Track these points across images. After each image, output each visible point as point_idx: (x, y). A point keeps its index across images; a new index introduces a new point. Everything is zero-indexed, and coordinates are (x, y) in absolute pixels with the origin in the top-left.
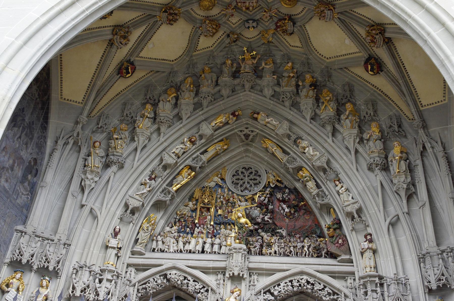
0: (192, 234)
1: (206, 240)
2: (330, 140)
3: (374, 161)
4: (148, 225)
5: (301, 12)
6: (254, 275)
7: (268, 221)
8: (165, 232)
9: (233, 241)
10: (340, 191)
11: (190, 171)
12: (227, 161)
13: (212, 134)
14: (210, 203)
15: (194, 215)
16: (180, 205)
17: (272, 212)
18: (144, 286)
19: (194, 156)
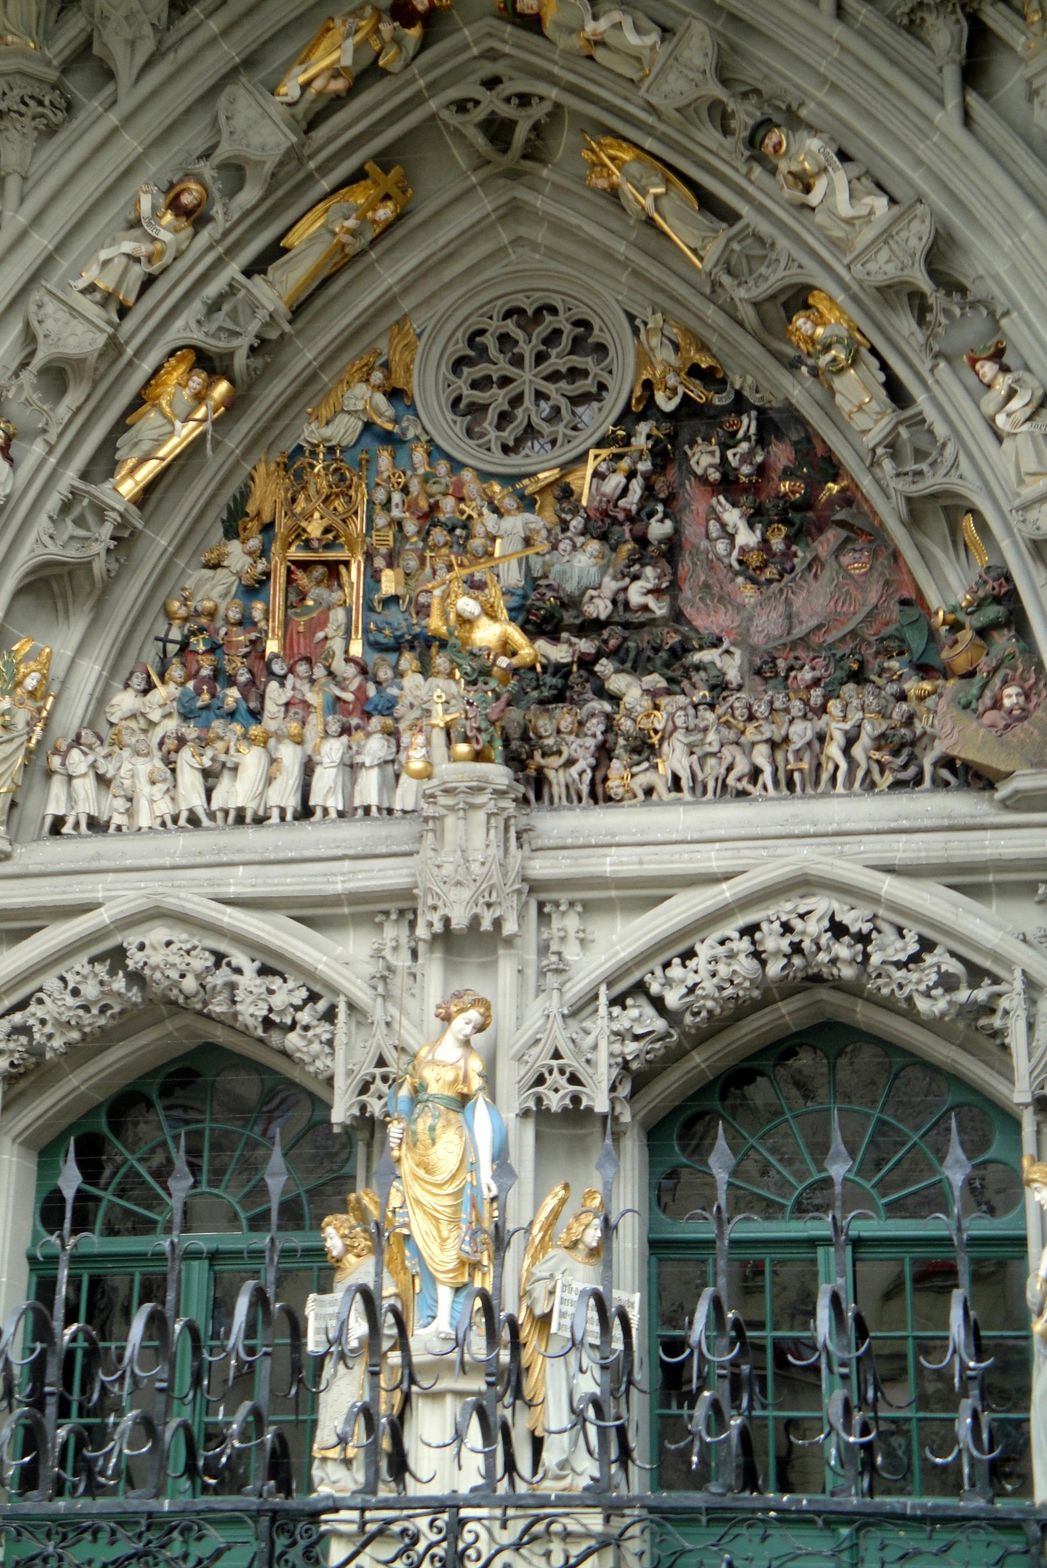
0: (256, 715)
1: (317, 750)
2: (948, 118)
6: (564, 913)
8: (114, 720)
10: (1001, 420)
11: (197, 380)
12: (408, 285)
13: (292, 148)
14: (336, 538)
15: (257, 614)
16: (181, 563)
18: (17, 1018)
19: (212, 290)
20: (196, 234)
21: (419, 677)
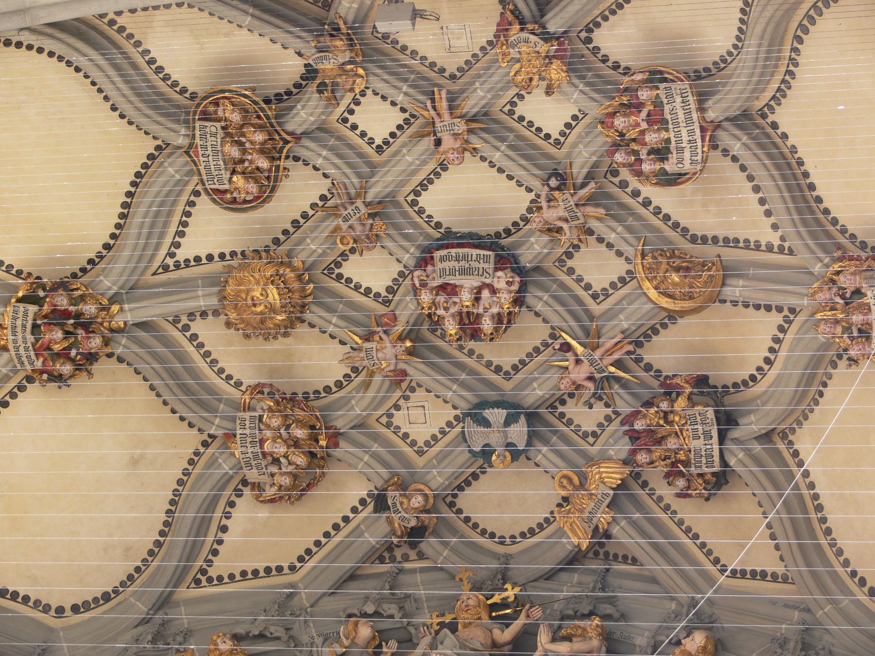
5: (768, 361)
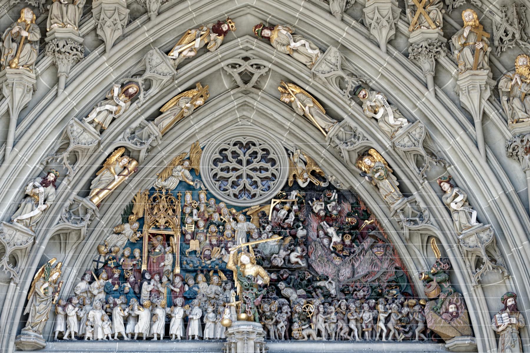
3: (522, 141)
4: (46, 285)
7: (297, 263)
8: (78, 293)
9: (234, 316)
10: (453, 206)
17: (306, 242)
20: (131, 104)
21: (206, 284)
